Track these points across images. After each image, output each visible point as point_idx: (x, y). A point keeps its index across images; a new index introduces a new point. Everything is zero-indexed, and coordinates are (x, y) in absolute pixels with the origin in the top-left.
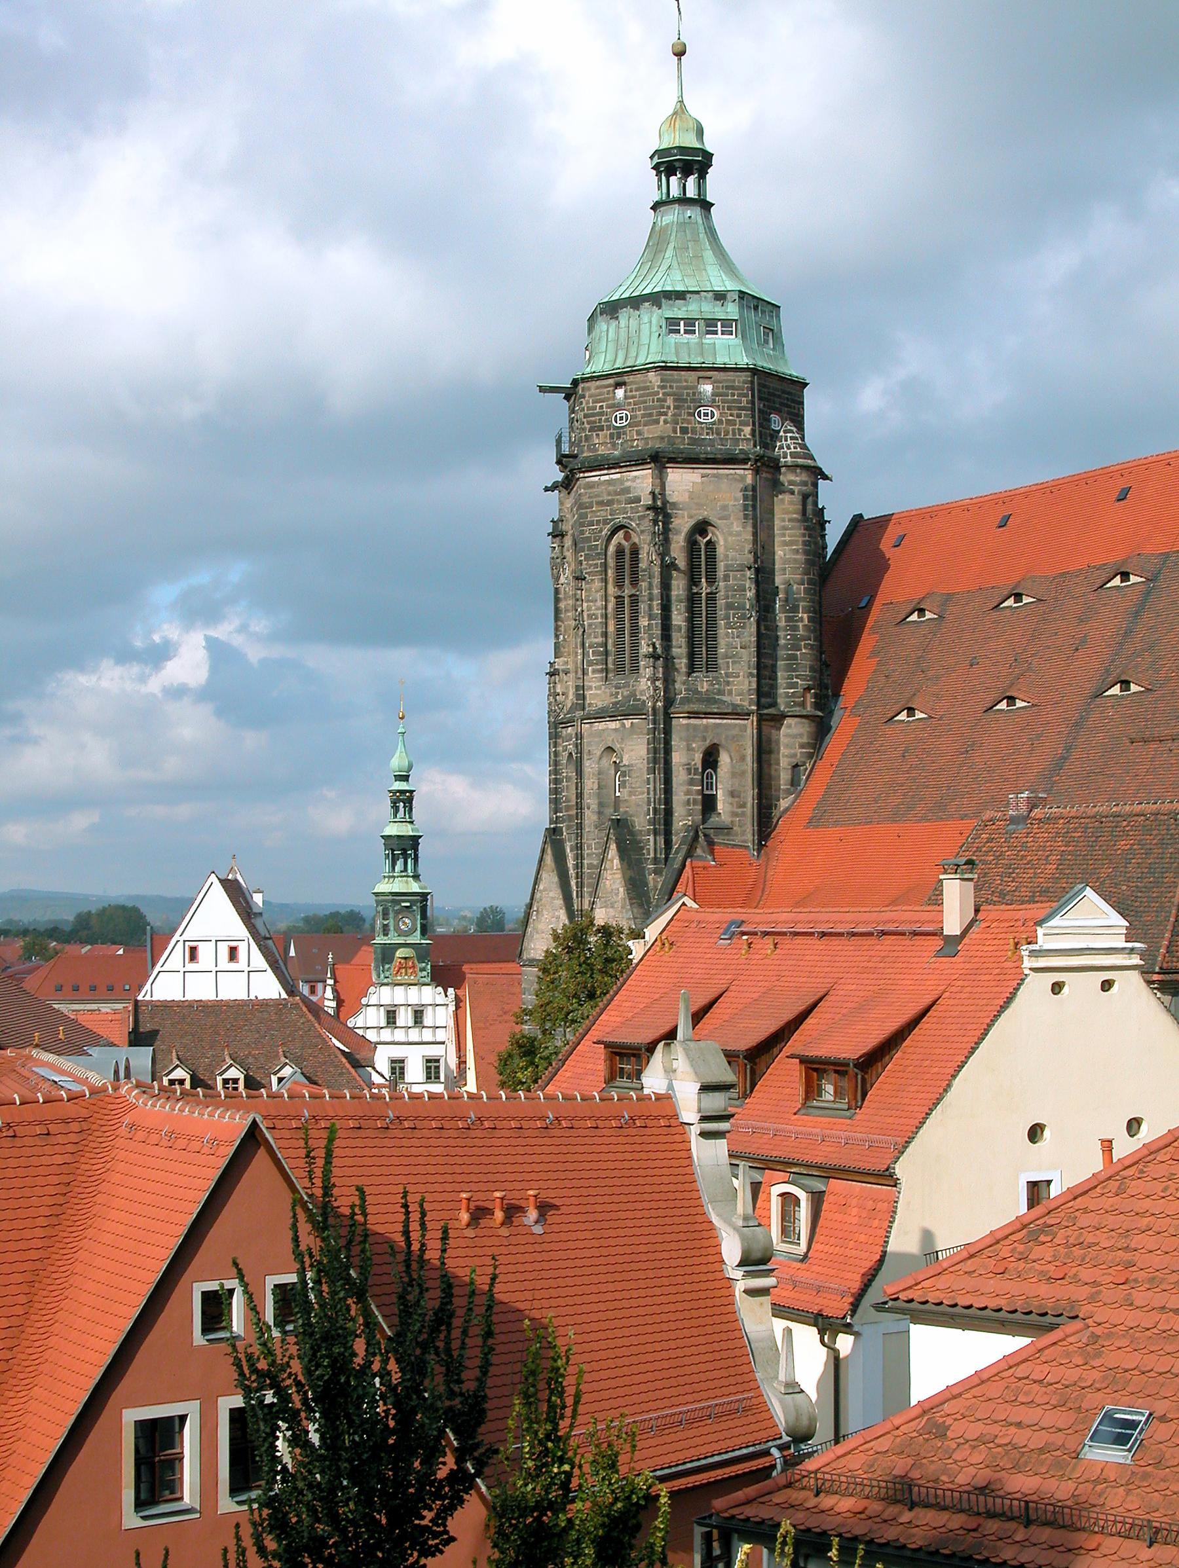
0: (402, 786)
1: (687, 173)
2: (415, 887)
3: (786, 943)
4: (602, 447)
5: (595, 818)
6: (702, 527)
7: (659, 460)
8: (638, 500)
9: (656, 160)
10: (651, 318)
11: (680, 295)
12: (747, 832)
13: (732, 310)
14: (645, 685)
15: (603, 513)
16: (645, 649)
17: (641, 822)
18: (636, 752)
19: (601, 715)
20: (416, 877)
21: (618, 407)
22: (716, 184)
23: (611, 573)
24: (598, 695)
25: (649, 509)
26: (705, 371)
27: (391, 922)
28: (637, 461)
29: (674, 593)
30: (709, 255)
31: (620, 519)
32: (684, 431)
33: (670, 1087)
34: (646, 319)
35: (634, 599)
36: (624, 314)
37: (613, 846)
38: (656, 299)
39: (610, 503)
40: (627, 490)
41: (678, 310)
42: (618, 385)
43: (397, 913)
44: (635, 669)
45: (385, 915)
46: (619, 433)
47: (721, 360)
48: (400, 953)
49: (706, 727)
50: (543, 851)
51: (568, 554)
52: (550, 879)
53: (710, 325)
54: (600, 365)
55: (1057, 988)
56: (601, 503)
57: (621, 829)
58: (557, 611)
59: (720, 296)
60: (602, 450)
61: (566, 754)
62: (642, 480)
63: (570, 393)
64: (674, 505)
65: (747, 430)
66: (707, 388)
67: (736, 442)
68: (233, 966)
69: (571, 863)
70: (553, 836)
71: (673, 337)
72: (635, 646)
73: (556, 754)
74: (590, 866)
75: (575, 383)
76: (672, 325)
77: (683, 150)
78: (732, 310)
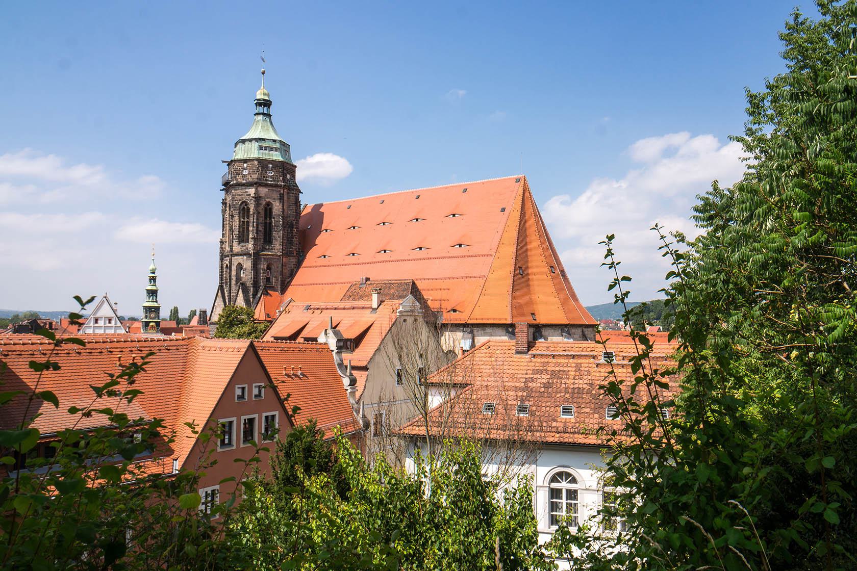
0: (153, 275)
1: (264, 106)
2: (156, 304)
3: (324, 311)
4: (240, 180)
5: (235, 282)
8: (250, 195)
9: (256, 101)
10: (255, 145)
11: (264, 140)
13: (278, 145)
14: (250, 246)
15: (239, 198)
16: (251, 236)
17: (249, 284)
18: (247, 264)
19: (237, 255)
20: (156, 302)
21: (244, 169)
22: (273, 110)
23: (241, 215)
24: (237, 248)
25: (253, 197)
28: (250, 185)
29: (259, 221)
30: (271, 129)
31: (244, 200)
32: (264, 177)
33: (327, 340)
34: (253, 144)
35: (248, 223)
36: (247, 143)
37: (241, 290)
39: (241, 195)
40: (247, 192)
41: (263, 144)
42: (244, 163)
43: (150, 312)
44: (248, 242)
46: (244, 176)
47: (275, 158)
48: (151, 324)
49: (268, 258)
50: (218, 291)
51: (228, 209)
52: (220, 299)
53: (271, 149)
54: (239, 156)
55: (405, 321)
56: (239, 195)
57: (243, 286)
58: (223, 224)
59: (274, 141)
60: (239, 180)
61: (225, 265)
62: (252, 191)
63: (230, 163)
64: (260, 197)
65: (281, 178)
66: (271, 166)
67: (278, 181)
68: (110, 325)
69: (226, 294)
70: (221, 288)
71: (261, 151)
72: (248, 235)
73: (222, 264)
74: (233, 296)
75: (232, 161)
76: (261, 148)
77: (264, 100)
78: (278, 145)
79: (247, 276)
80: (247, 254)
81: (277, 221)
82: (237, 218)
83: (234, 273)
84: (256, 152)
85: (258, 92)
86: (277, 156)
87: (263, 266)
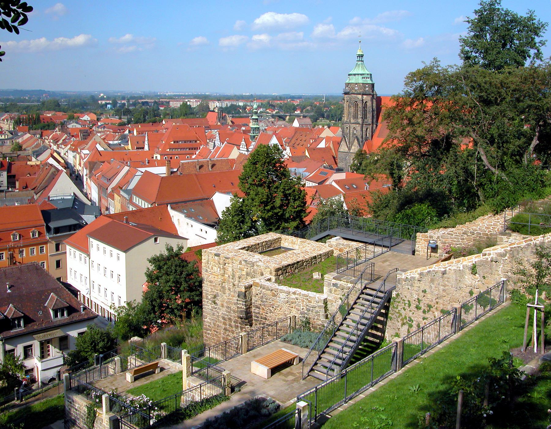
6: (366, 102)
7: (363, 95)
10: (360, 77)
12: (370, 138)
14: (360, 121)
17: (360, 137)
18: (358, 128)
19: (353, 124)
22: (364, 58)
24: (352, 121)
26: (367, 84)
27: (254, 132)
36: (356, 76)
38: (361, 74)
45: (254, 131)
47: (369, 82)
59: (368, 74)
79: (359, 134)
80: (359, 124)
81: (369, 109)
83: (351, 132)
84: (361, 80)
85: (359, 51)
86: (369, 81)
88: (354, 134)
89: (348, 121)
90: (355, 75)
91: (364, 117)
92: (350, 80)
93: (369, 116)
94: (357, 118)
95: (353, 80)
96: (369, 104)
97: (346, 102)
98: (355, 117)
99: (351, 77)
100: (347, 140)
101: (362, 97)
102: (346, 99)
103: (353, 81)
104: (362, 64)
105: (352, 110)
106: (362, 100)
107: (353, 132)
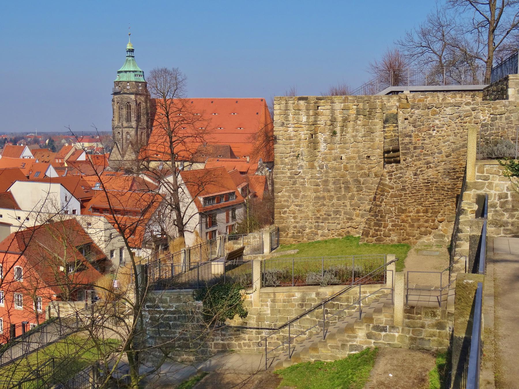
11: (136, 71)
14: (134, 124)
18: (133, 132)
19: (126, 127)
24: (125, 124)
31: (128, 101)
36: (128, 73)
38: (133, 72)
41: (136, 73)
46: (128, 89)
59: (140, 72)
62: (133, 97)
66: (140, 84)
80: (132, 128)
82: (125, 110)
83: (124, 137)
85: (128, 45)
86: (142, 80)
87: (139, 133)
88: (127, 139)
89: (120, 124)
90: (126, 72)
91: (138, 120)
92: (120, 78)
93: (143, 119)
94: (131, 121)
95: (124, 78)
96: (143, 105)
97: (116, 104)
98: (128, 120)
99: (121, 74)
100: (119, 147)
101: (136, 97)
102: (115, 100)
103: (124, 79)
104: (133, 60)
105: (124, 112)
106: (136, 101)
107: (126, 137)
